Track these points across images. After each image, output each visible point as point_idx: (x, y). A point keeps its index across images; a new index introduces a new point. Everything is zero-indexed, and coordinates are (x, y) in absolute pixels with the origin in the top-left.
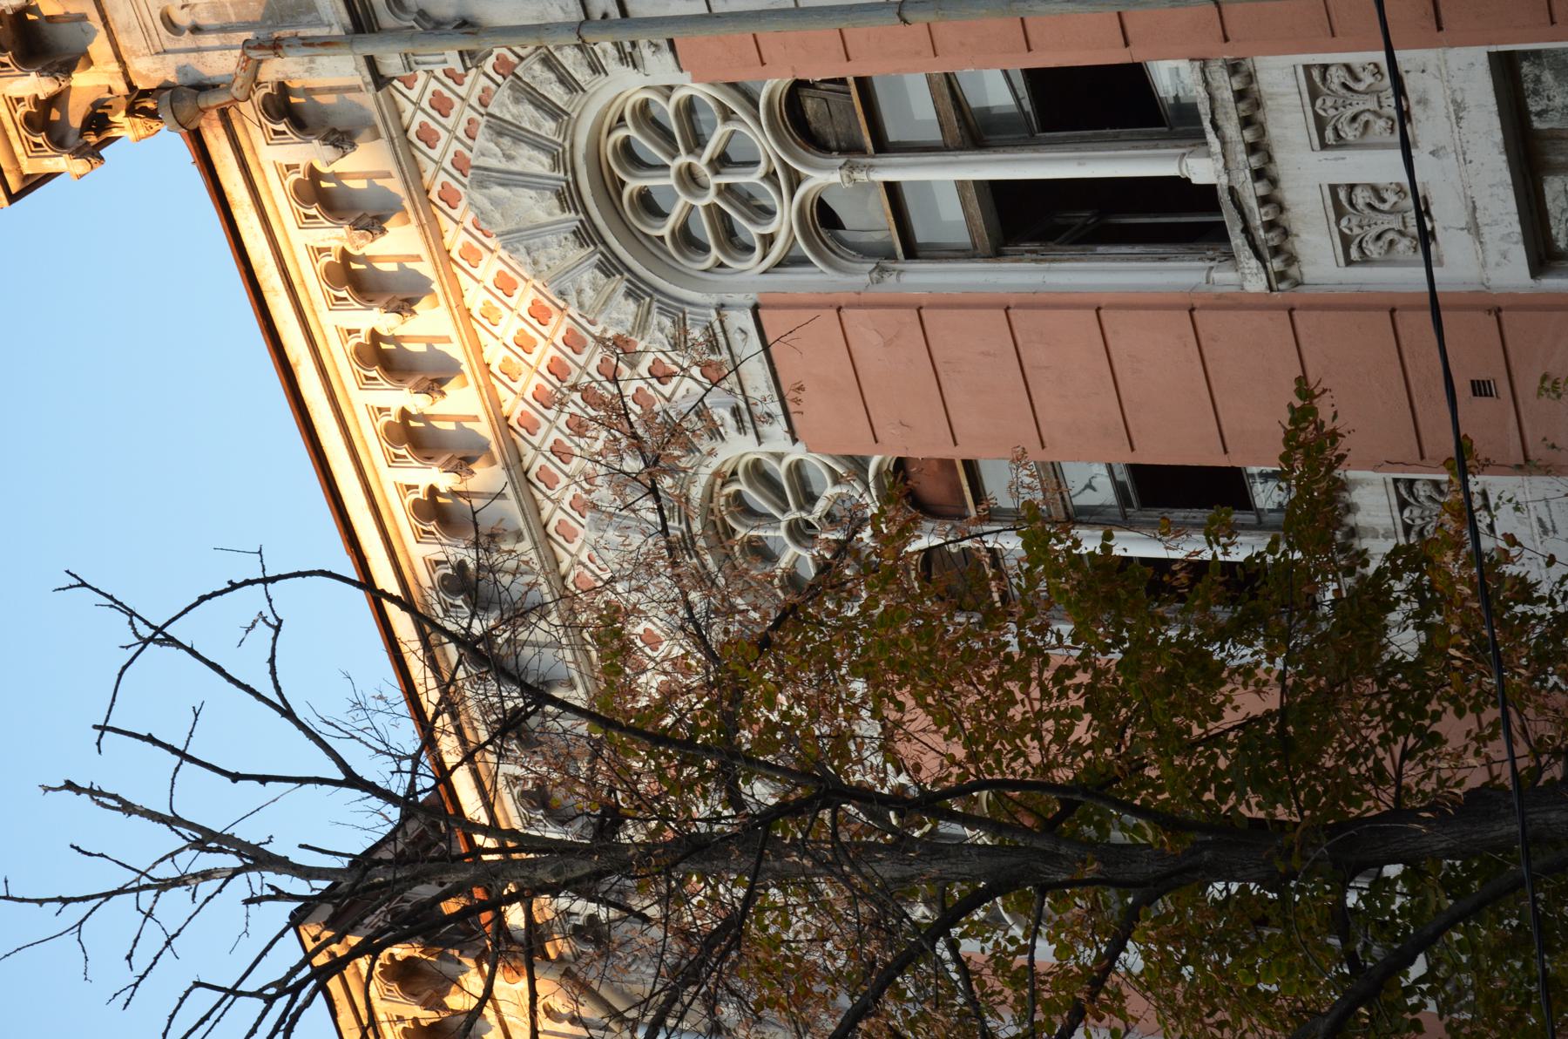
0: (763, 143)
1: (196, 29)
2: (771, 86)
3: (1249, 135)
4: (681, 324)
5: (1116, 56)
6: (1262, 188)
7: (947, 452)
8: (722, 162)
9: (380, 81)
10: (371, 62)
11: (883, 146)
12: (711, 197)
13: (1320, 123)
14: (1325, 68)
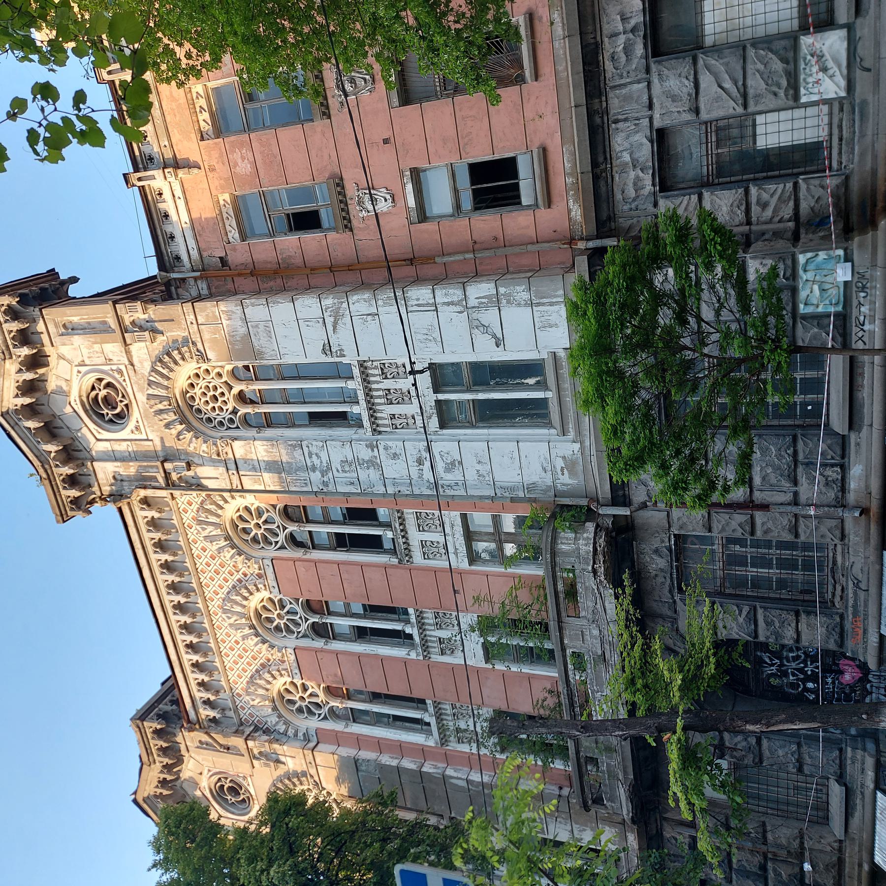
0: (277, 519)
1: (122, 480)
2: (280, 506)
5: (371, 507)
7: (321, 599)
8: (266, 522)
9: (173, 498)
10: (172, 494)
11: (308, 521)
12: (262, 531)
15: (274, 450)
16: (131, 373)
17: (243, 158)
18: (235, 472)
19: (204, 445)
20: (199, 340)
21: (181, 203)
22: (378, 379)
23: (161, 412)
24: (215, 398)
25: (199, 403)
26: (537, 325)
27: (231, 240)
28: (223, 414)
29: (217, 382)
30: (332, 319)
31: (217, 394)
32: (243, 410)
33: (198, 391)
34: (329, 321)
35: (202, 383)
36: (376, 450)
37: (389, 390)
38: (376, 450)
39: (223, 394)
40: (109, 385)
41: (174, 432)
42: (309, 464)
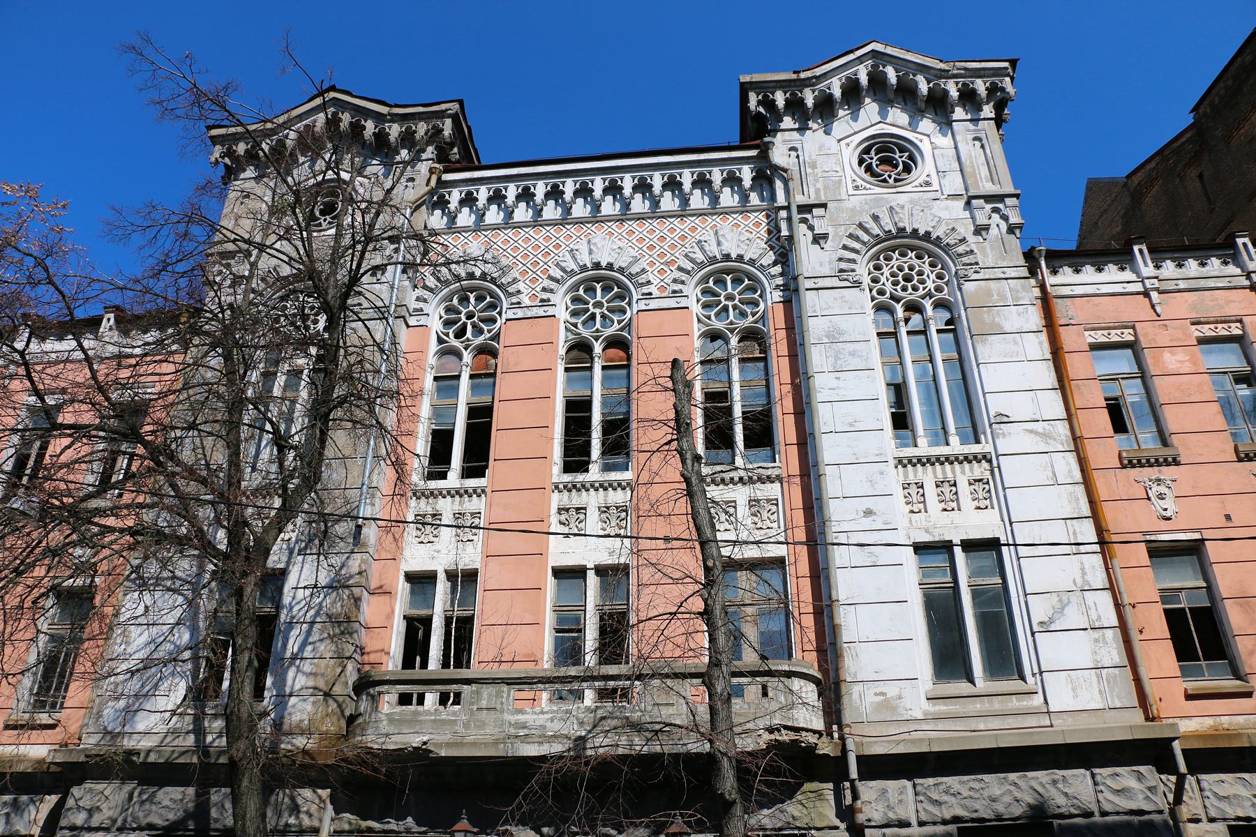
4: (683, 282)
6: (736, 479)
14: (777, 505)
16: (933, 195)
17: (1182, 362)
20: (987, 277)
21: (1118, 288)
24: (908, 279)
26: (1076, 675)
27: (1087, 333)
28: (889, 284)
29: (930, 285)
30: (1040, 430)
31: (915, 282)
32: (900, 312)
33: (915, 262)
34: (1038, 427)
35: (927, 269)
37: (955, 485)
39: (915, 289)
40: (907, 169)
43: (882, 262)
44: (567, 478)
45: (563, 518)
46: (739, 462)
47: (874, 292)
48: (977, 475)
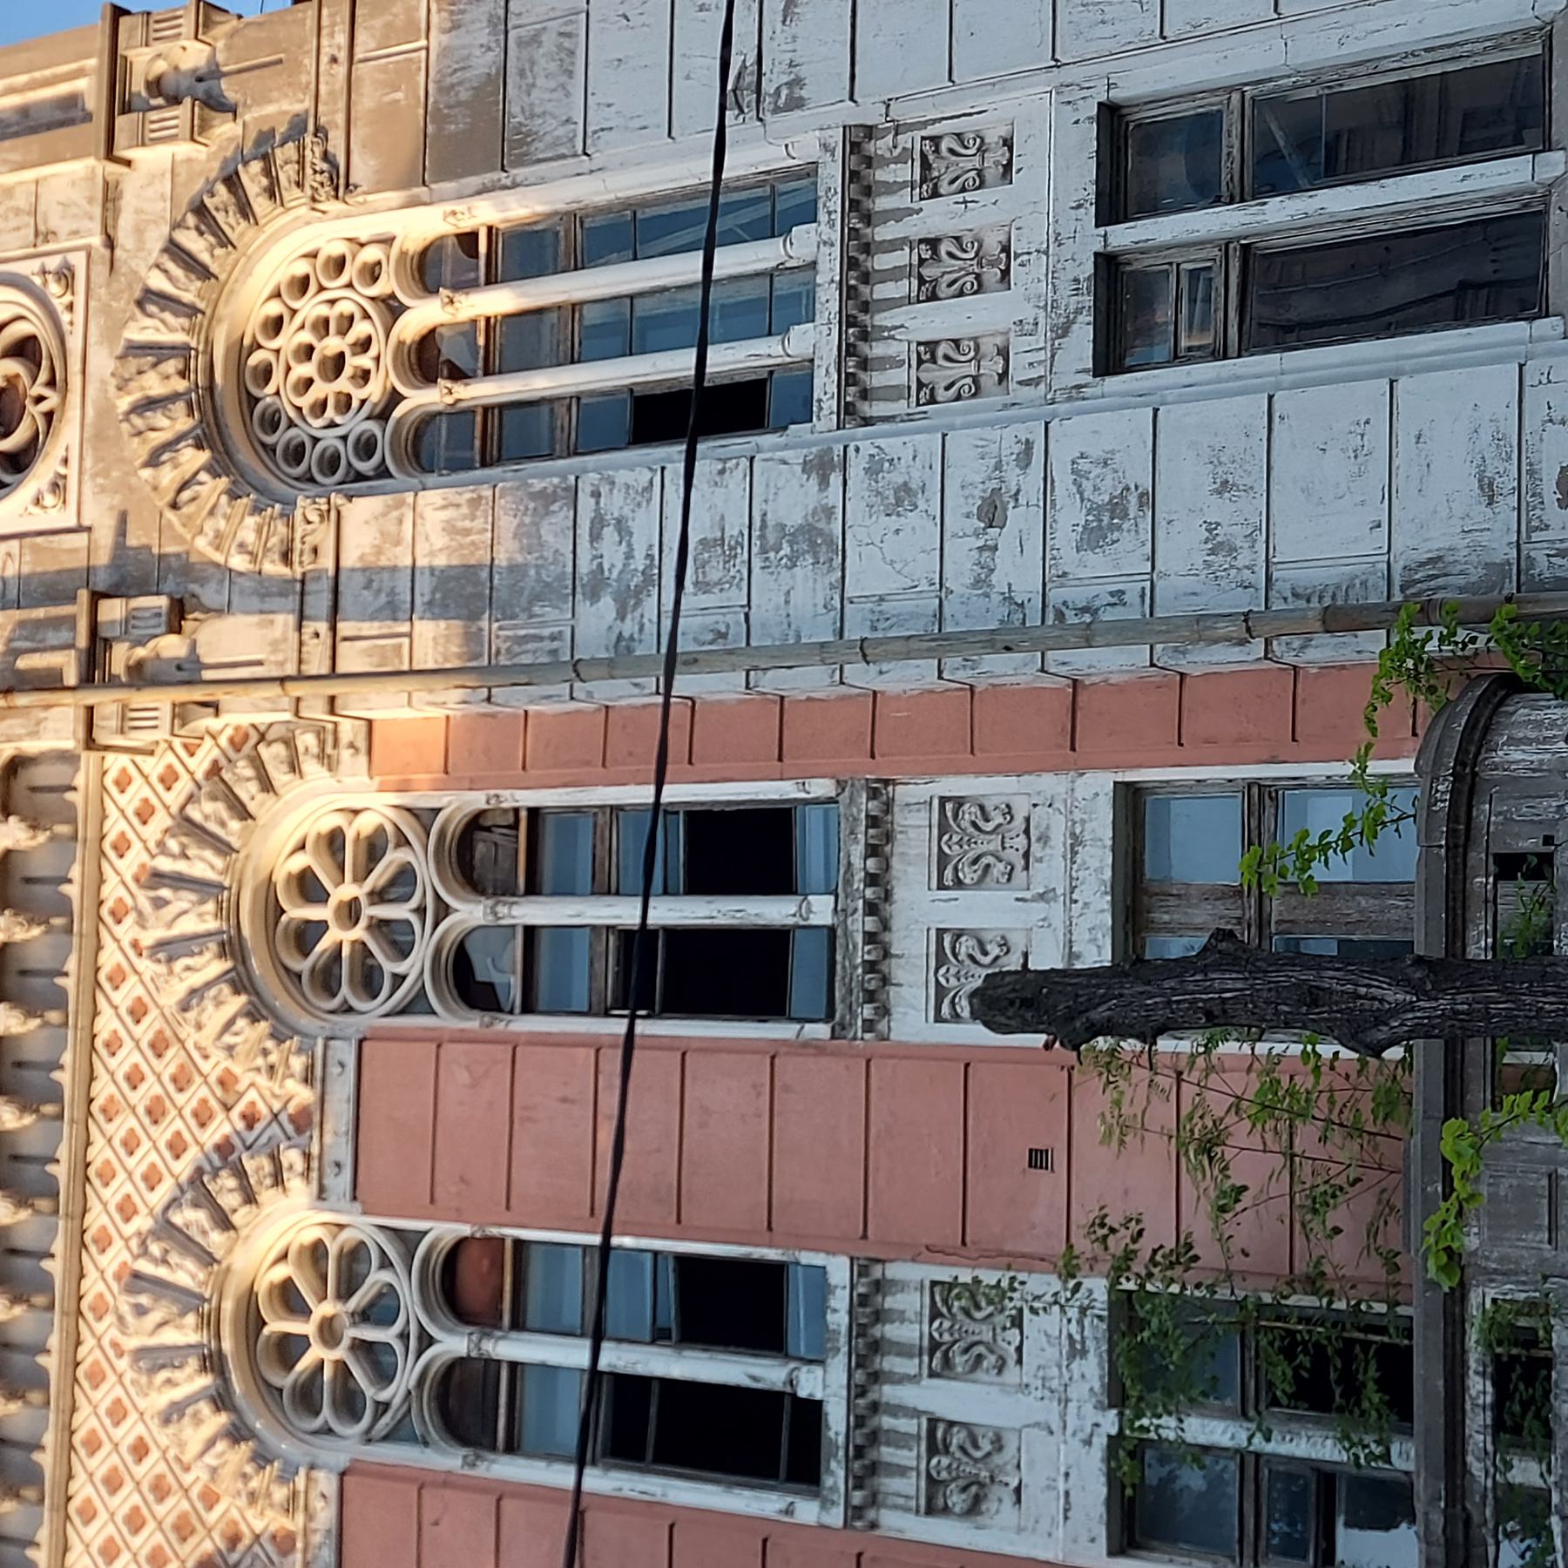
3: (871, 863)
13: (943, 859)
14: (959, 802)
15: (478, 523)
18: (323, 627)
19: (251, 521)
22: (902, 200)
23: (150, 404)
25: (279, 393)
36: (835, 479)
38: (835, 479)
41: (168, 477)
42: (584, 567)
43: (281, 438)
44: (835, 1475)
45: (957, 1500)
46: (821, 910)
47: (365, 467)
48: (906, 172)
